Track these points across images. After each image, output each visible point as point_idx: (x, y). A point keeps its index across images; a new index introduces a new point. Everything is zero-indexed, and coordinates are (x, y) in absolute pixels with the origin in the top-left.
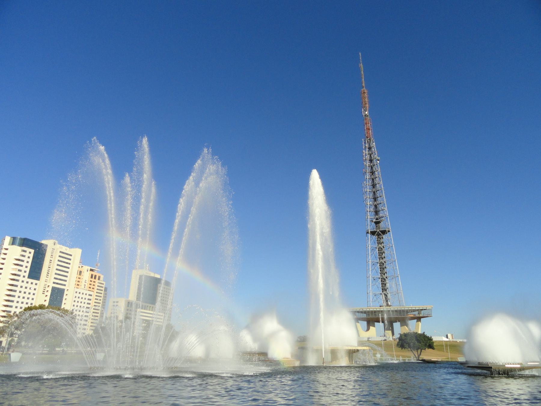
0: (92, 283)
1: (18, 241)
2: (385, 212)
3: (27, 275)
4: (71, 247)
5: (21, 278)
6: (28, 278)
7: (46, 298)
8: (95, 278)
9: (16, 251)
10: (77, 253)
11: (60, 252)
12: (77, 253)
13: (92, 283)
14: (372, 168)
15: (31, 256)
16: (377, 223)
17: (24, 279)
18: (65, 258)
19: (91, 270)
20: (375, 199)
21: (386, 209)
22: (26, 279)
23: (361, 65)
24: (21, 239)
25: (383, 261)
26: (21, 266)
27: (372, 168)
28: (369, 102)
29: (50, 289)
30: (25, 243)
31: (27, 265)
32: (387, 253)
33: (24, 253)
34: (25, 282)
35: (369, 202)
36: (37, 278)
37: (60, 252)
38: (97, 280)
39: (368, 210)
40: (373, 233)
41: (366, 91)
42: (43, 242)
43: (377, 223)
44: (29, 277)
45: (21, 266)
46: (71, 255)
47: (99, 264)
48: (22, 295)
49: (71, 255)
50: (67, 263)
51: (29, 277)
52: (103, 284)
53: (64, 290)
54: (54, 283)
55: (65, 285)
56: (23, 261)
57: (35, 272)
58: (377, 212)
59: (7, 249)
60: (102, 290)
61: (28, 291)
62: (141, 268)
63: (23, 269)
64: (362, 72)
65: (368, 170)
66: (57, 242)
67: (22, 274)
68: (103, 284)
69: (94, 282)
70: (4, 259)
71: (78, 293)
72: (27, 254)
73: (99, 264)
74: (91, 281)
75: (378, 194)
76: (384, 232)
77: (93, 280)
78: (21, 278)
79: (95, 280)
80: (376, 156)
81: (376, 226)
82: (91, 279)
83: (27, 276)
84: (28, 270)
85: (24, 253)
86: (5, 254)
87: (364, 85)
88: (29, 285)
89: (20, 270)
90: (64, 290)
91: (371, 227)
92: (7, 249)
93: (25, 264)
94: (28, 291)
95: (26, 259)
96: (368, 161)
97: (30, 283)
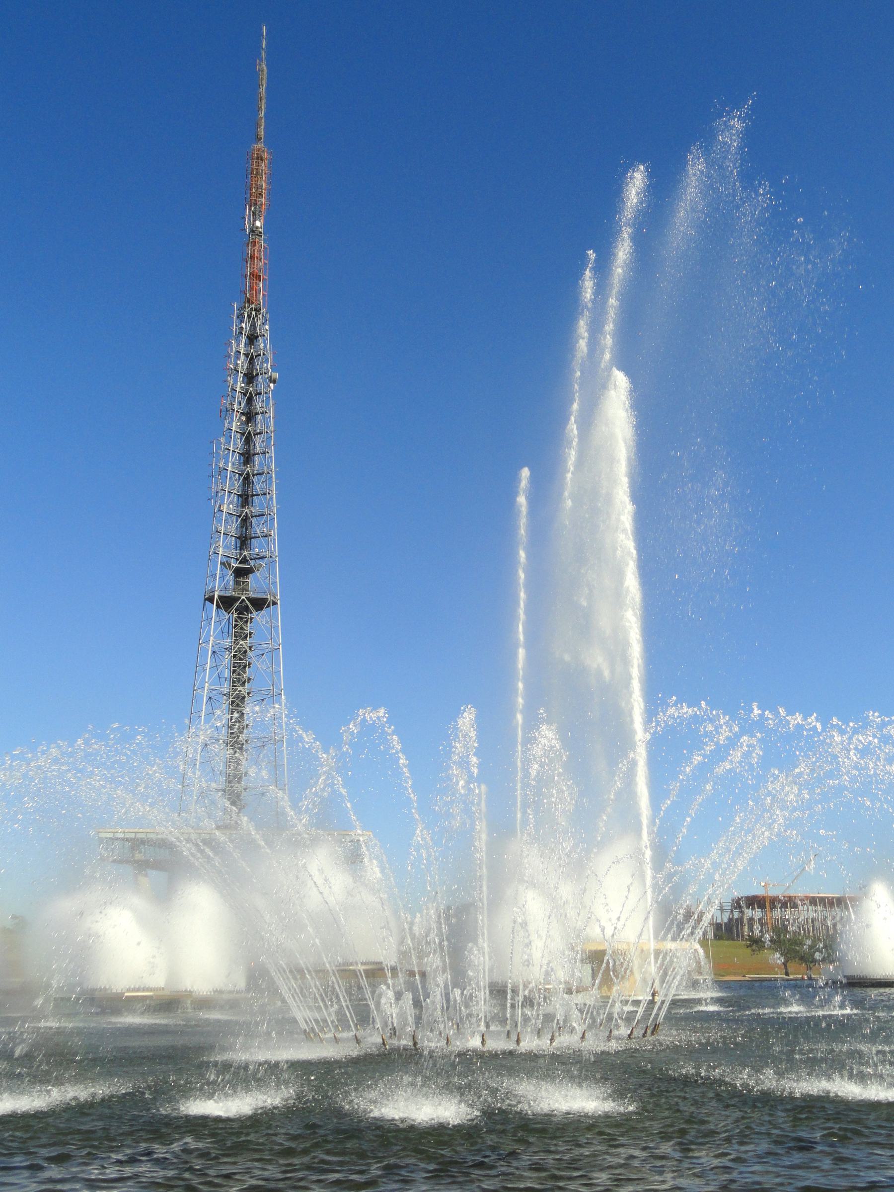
2: (271, 542)
14: (250, 401)
16: (241, 573)
20: (245, 499)
21: (274, 533)
23: (264, 65)
25: (243, 690)
27: (250, 401)
28: (269, 192)
32: (258, 666)
35: (229, 505)
39: (222, 530)
40: (226, 603)
41: (265, 156)
43: (241, 573)
58: (244, 541)
64: (263, 90)
65: (239, 404)
75: (258, 486)
76: (259, 604)
80: (266, 366)
81: (237, 583)
87: (262, 132)
91: (222, 583)
96: (240, 377)
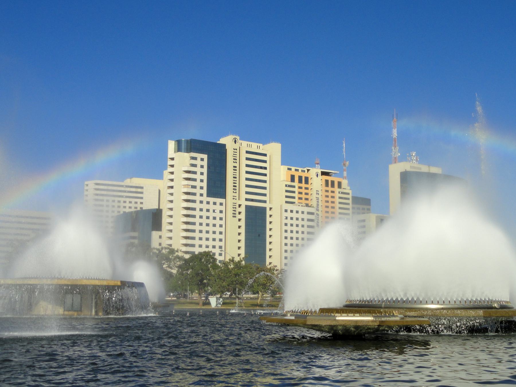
0: (330, 194)
1: (183, 146)
3: (204, 191)
4: (264, 143)
5: (198, 198)
6: (207, 196)
7: (240, 224)
8: (333, 185)
9: (182, 161)
10: (273, 150)
11: (247, 152)
12: (273, 150)
13: (330, 194)
15: (205, 163)
17: (201, 198)
18: (257, 160)
19: (323, 173)
22: (205, 198)
24: (187, 141)
26: (195, 180)
29: (243, 209)
30: (193, 146)
31: (202, 177)
33: (194, 162)
34: (205, 202)
36: (222, 195)
37: (247, 152)
38: (336, 189)
42: (222, 141)
44: (209, 195)
45: (195, 180)
46: (265, 155)
47: (347, 163)
48: (204, 221)
49: (265, 155)
50: (261, 168)
51: (209, 195)
52: (348, 194)
53: (264, 209)
54: (247, 200)
55: (265, 202)
56: (195, 173)
57: (217, 186)
59: (172, 159)
60: (348, 204)
61: (211, 214)
62: (403, 158)
63: (198, 184)
66: (238, 138)
67: (198, 191)
68: (348, 194)
69: (333, 192)
70: (172, 173)
71: (289, 211)
72: (198, 162)
73: (347, 163)
74: (327, 191)
77: (330, 189)
78: (198, 198)
79: (333, 189)
82: (327, 189)
83: (205, 195)
84: (205, 184)
85: (194, 162)
86: (172, 166)
88: (211, 207)
89: (194, 187)
90: (264, 209)
92: (172, 159)
93: (198, 177)
94: (211, 214)
95: (198, 169)
97: (211, 203)
